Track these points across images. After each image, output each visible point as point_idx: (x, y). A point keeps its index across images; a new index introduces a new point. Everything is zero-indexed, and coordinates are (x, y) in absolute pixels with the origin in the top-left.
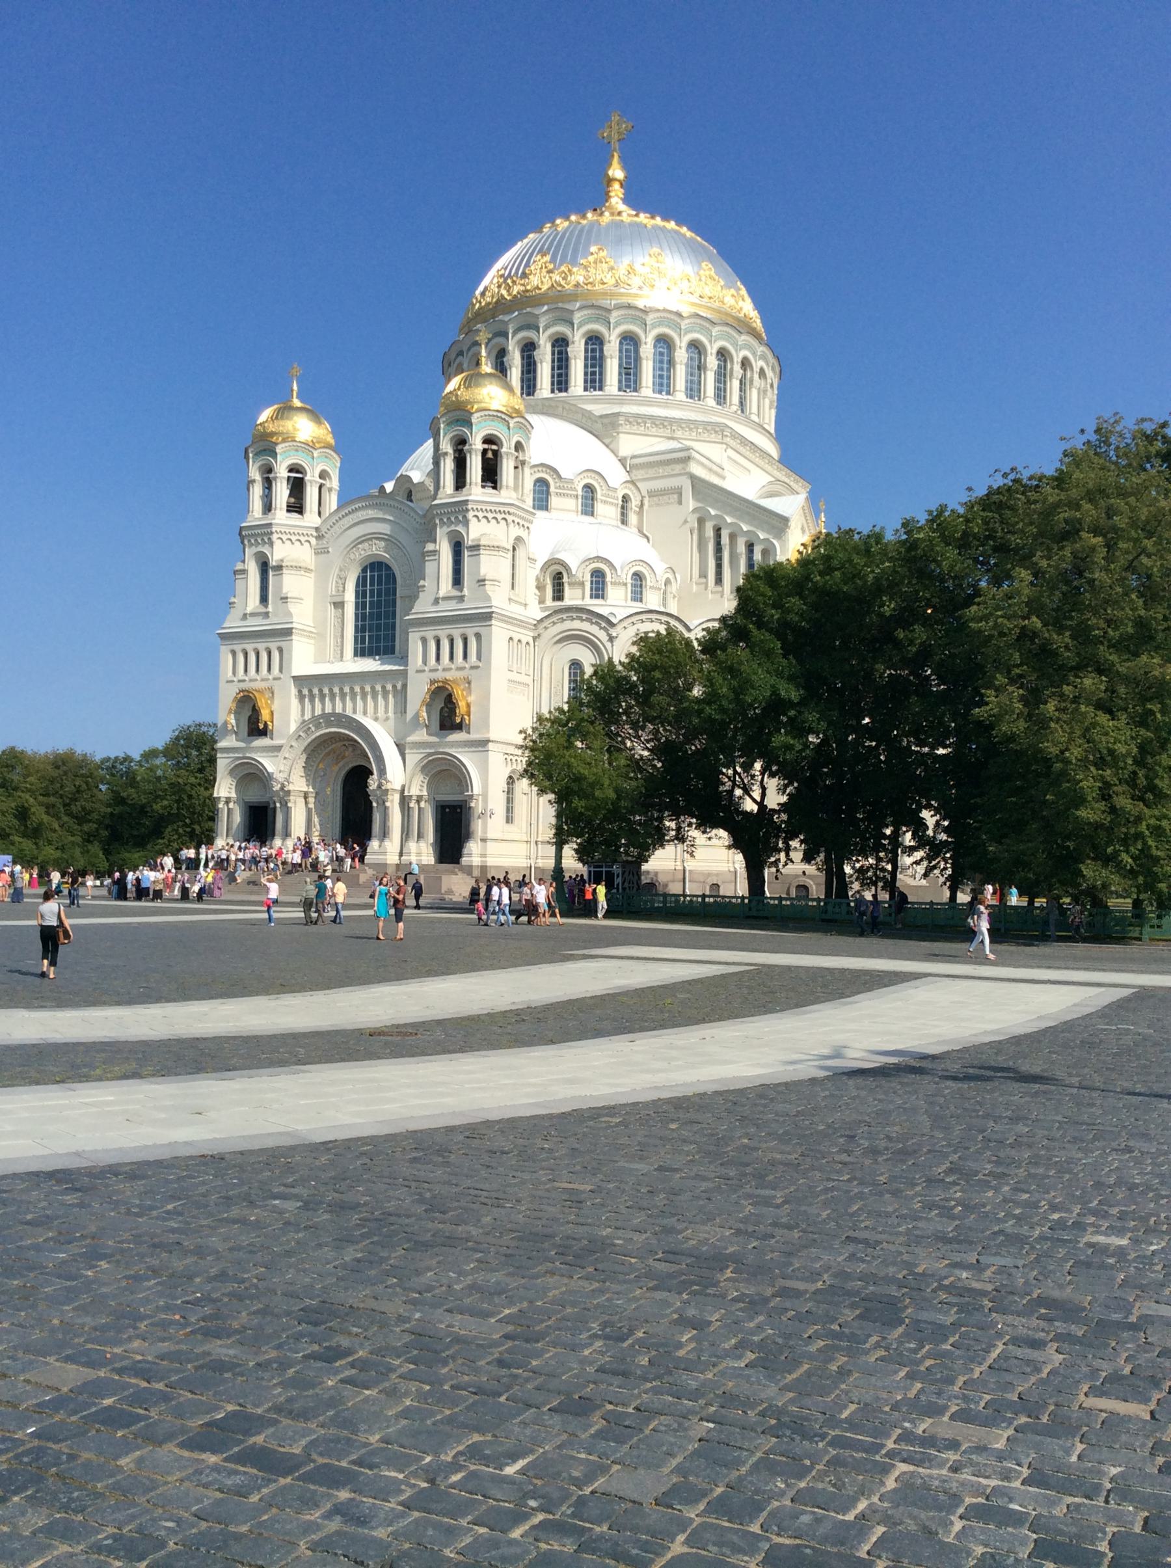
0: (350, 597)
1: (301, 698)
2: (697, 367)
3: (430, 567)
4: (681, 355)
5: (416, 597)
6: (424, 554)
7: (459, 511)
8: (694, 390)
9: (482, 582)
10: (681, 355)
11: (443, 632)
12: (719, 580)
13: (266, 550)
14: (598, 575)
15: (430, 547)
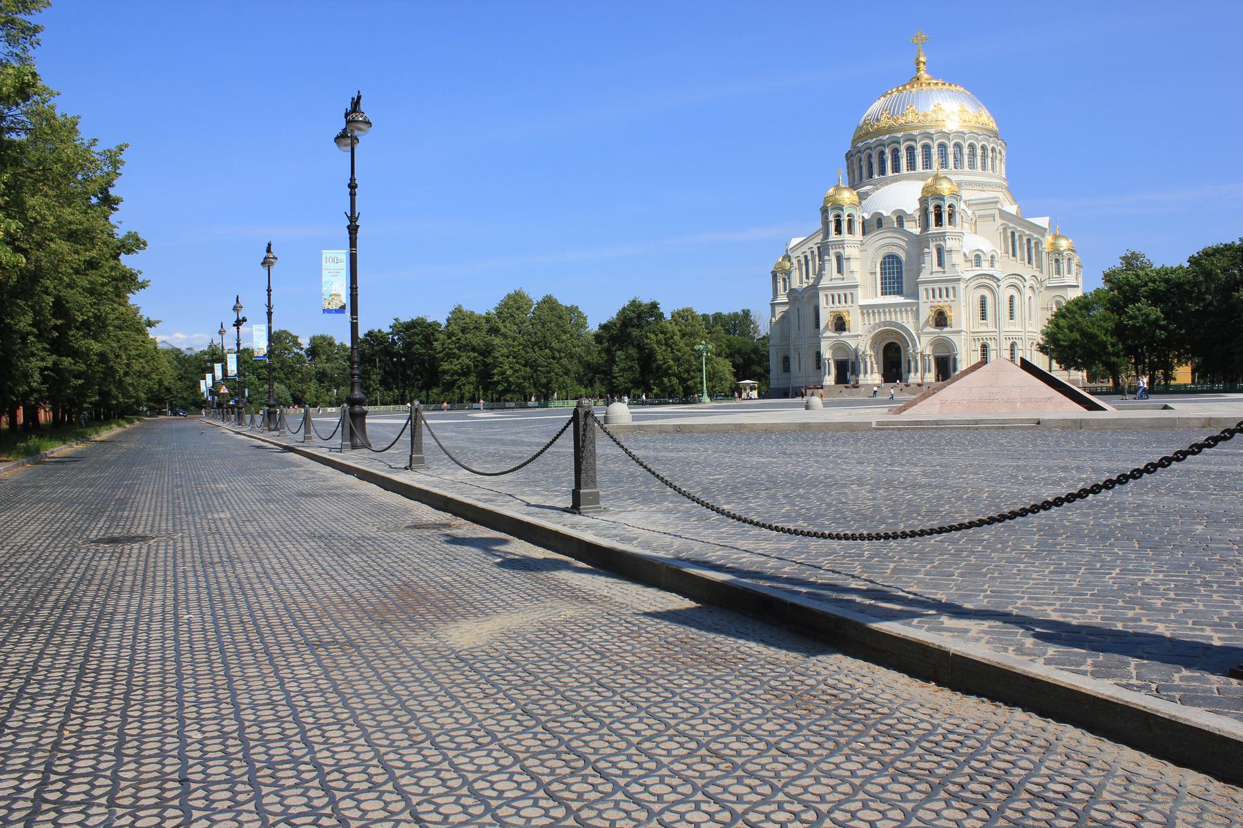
0: (878, 270)
1: (863, 314)
2: (984, 156)
3: (927, 259)
4: (979, 152)
5: (919, 272)
6: (923, 254)
7: (942, 236)
8: (972, 165)
9: (954, 265)
10: (979, 152)
11: (936, 286)
12: (1014, 255)
13: (841, 251)
14: (978, 257)
15: (926, 250)
